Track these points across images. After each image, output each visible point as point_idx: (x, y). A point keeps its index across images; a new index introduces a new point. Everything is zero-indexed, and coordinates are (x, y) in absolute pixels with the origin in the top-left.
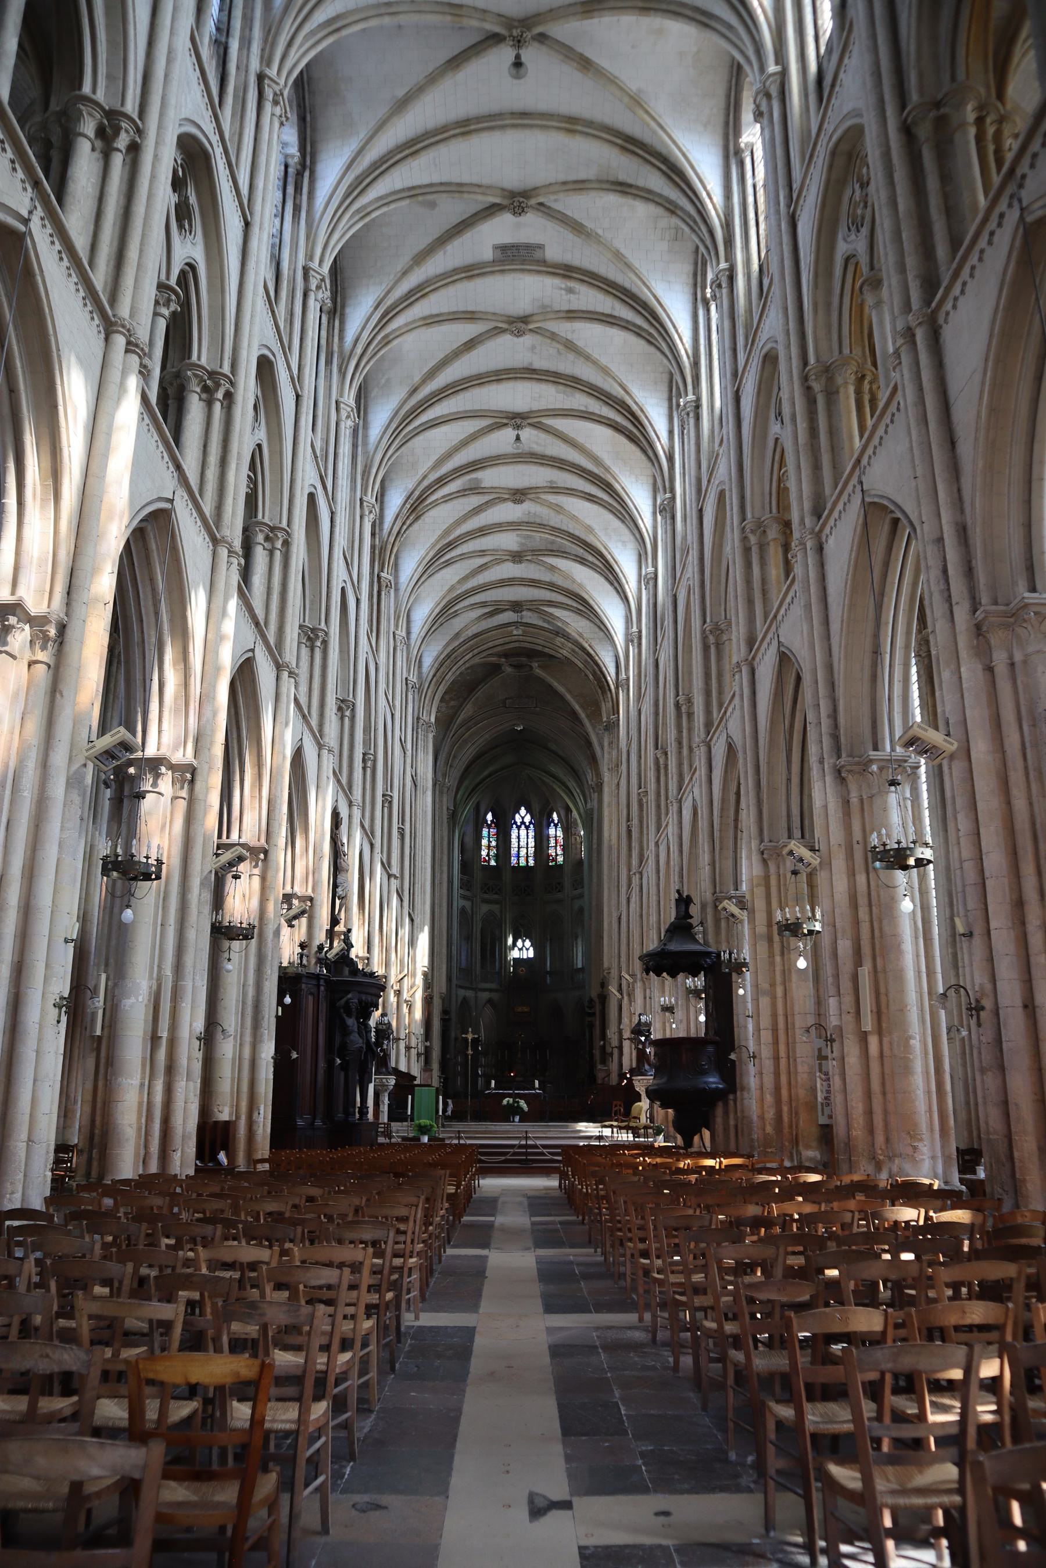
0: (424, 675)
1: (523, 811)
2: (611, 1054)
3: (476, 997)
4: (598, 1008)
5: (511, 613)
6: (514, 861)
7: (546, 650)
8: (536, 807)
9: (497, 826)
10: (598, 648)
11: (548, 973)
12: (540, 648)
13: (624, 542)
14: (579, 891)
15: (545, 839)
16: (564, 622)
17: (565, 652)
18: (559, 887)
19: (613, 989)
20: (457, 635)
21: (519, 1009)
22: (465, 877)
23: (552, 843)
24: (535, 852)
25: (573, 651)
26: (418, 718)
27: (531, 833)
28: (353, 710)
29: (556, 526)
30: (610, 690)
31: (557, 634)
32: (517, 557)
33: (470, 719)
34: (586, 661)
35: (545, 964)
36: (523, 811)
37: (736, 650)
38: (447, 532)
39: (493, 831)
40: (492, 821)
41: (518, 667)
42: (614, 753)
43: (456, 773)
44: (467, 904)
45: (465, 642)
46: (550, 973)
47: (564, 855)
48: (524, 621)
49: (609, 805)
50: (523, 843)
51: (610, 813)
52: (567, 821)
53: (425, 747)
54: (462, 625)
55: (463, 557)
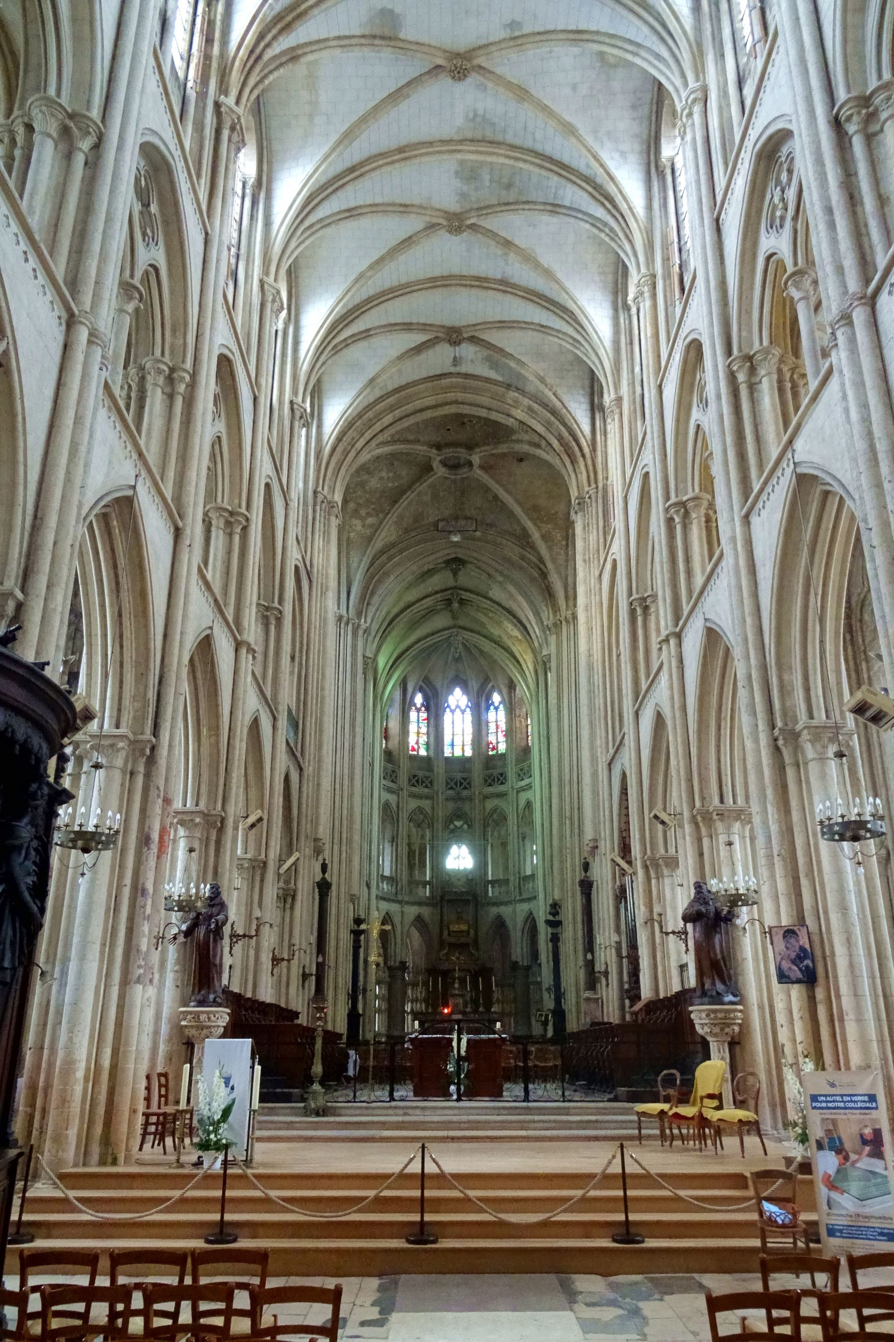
1: (458, 691)
2: (606, 974)
3: (402, 912)
5: (447, 346)
6: (447, 753)
7: (494, 416)
8: (474, 685)
9: (428, 709)
10: (566, 398)
12: (483, 413)
13: (623, 154)
16: (519, 362)
17: (519, 414)
18: (501, 778)
20: (372, 380)
21: (455, 928)
23: (492, 728)
24: (473, 740)
25: (530, 409)
26: (315, 492)
28: (97, 146)
29: (517, 142)
30: (583, 456)
31: (509, 386)
33: (393, 545)
35: (486, 874)
36: (458, 691)
39: (424, 715)
40: (423, 705)
41: (453, 466)
42: (593, 537)
43: (372, 620)
44: (392, 799)
46: (493, 882)
49: (587, 608)
50: (458, 730)
52: (511, 704)
55: (376, 209)
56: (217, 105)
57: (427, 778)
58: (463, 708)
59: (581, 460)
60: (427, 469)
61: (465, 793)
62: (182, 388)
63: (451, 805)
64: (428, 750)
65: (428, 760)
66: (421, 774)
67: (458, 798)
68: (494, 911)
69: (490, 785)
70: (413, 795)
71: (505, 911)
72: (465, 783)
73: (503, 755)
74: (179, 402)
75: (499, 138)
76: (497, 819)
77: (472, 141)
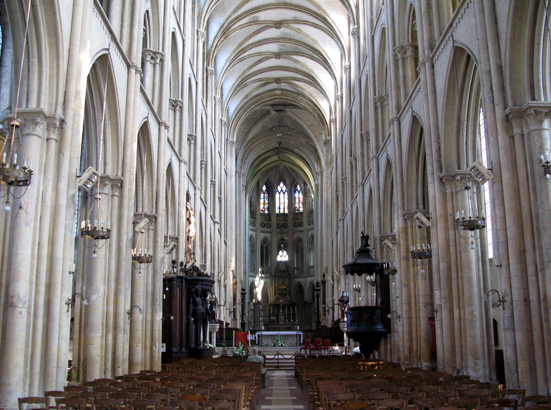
0: (230, 117)
4: (321, 287)
5: (275, 84)
6: (277, 211)
7: (293, 103)
8: (288, 182)
9: (268, 193)
11: (295, 268)
12: (290, 102)
14: (311, 226)
15: (293, 199)
17: (303, 104)
18: (301, 224)
19: (329, 278)
20: (247, 96)
22: (252, 220)
23: (297, 200)
24: (288, 206)
25: (308, 103)
26: (227, 140)
27: (286, 196)
29: (298, 40)
30: (327, 123)
32: (277, 56)
34: (314, 108)
35: (294, 264)
37: (391, 112)
38: (241, 44)
39: (266, 195)
40: (266, 190)
42: (329, 156)
43: (247, 166)
44: (254, 233)
45: (251, 99)
46: (297, 268)
47: (303, 207)
48: (282, 88)
49: (327, 183)
50: (282, 201)
51: (327, 187)
52: (305, 190)
53: (231, 154)
54: (249, 91)
56: (207, 69)
57: (268, 224)
58: (284, 191)
59: (326, 125)
60: (268, 112)
61: (285, 230)
62: (204, 166)
63: (279, 236)
64: (268, 211)
65: (269, 215)
66: (266, 222)
67: (282, 233)
68: (297, 280)
69: (296, 227)
70: (262, 232)
71: (302, 280)
72: (285, 226)
73: (302, 213)
74: (203, 170)
75: (292, 38)
76: (300, 240)
77: (283, 38)
